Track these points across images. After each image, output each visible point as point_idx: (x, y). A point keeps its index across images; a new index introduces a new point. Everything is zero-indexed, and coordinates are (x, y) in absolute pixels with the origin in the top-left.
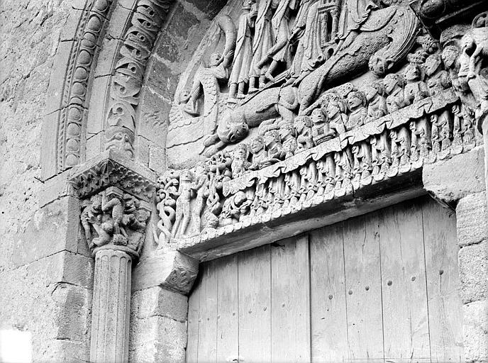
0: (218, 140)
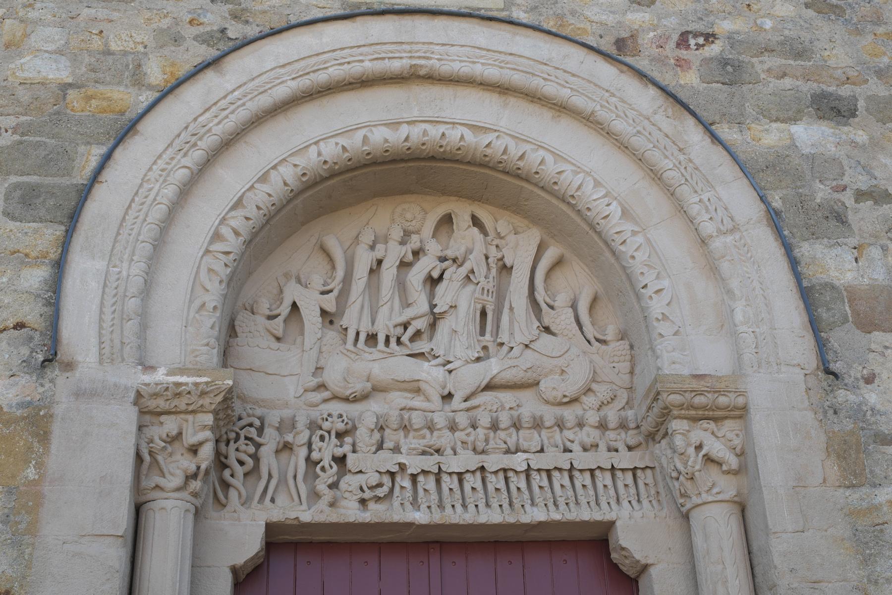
0: (322, 386)
